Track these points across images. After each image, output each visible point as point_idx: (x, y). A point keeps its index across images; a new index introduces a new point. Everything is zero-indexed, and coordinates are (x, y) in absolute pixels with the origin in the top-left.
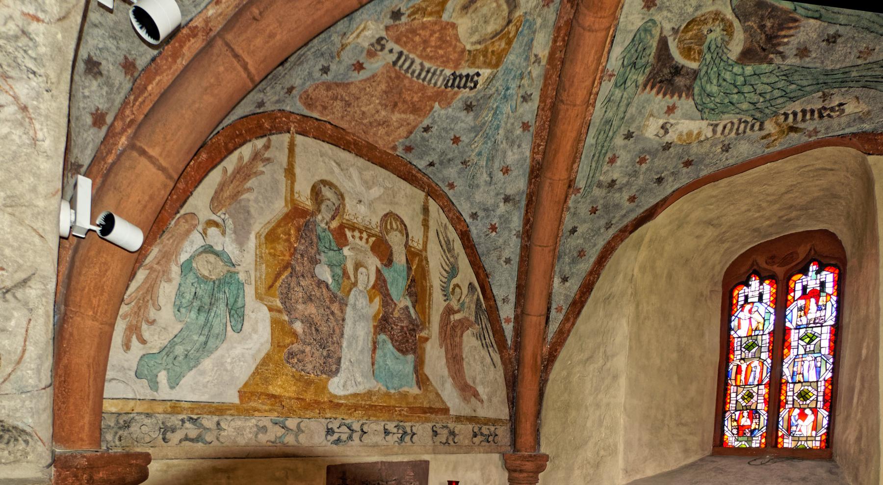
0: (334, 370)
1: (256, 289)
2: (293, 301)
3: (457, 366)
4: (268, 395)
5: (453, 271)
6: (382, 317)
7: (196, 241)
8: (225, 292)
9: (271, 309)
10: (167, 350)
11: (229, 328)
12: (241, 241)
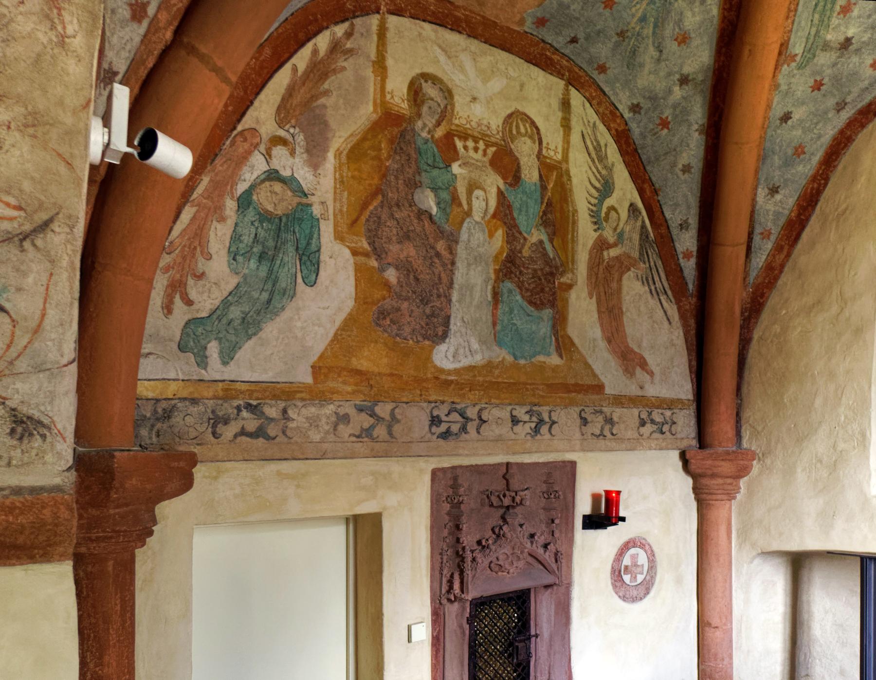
0: (440, 333)
1: (336, 226)
2: (384, 240)
3: (614, 324)
4: (352, 370)
5: (606, 189)
6: (506, 257)
7: (257, 165)
8: (294, 232)
9: (355, 253)
10: (219, 313)
11: (299, 280)
12: (315, 161)
